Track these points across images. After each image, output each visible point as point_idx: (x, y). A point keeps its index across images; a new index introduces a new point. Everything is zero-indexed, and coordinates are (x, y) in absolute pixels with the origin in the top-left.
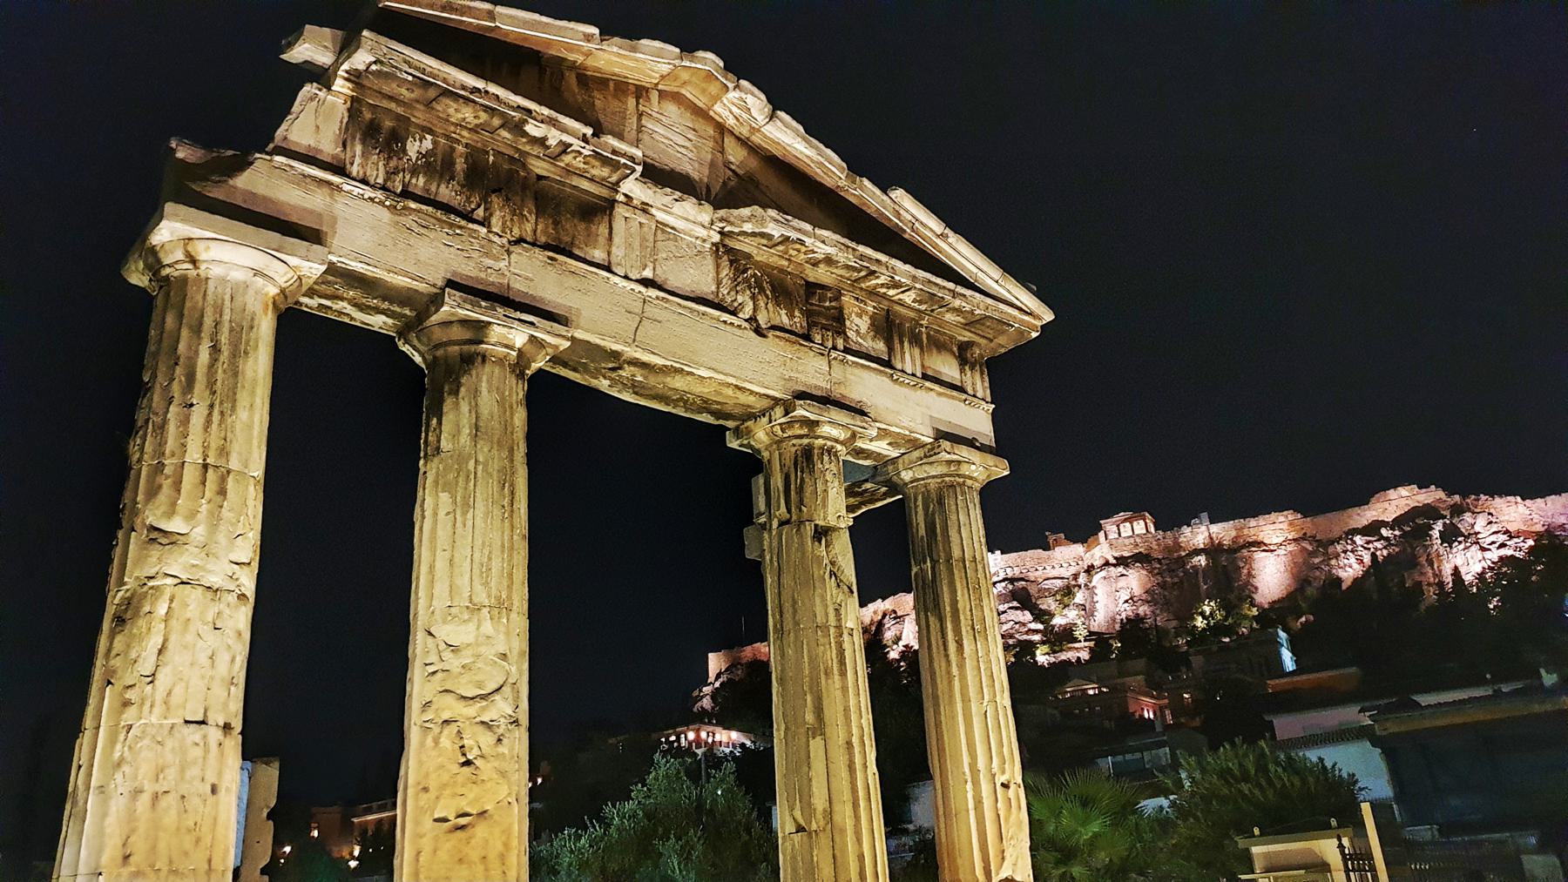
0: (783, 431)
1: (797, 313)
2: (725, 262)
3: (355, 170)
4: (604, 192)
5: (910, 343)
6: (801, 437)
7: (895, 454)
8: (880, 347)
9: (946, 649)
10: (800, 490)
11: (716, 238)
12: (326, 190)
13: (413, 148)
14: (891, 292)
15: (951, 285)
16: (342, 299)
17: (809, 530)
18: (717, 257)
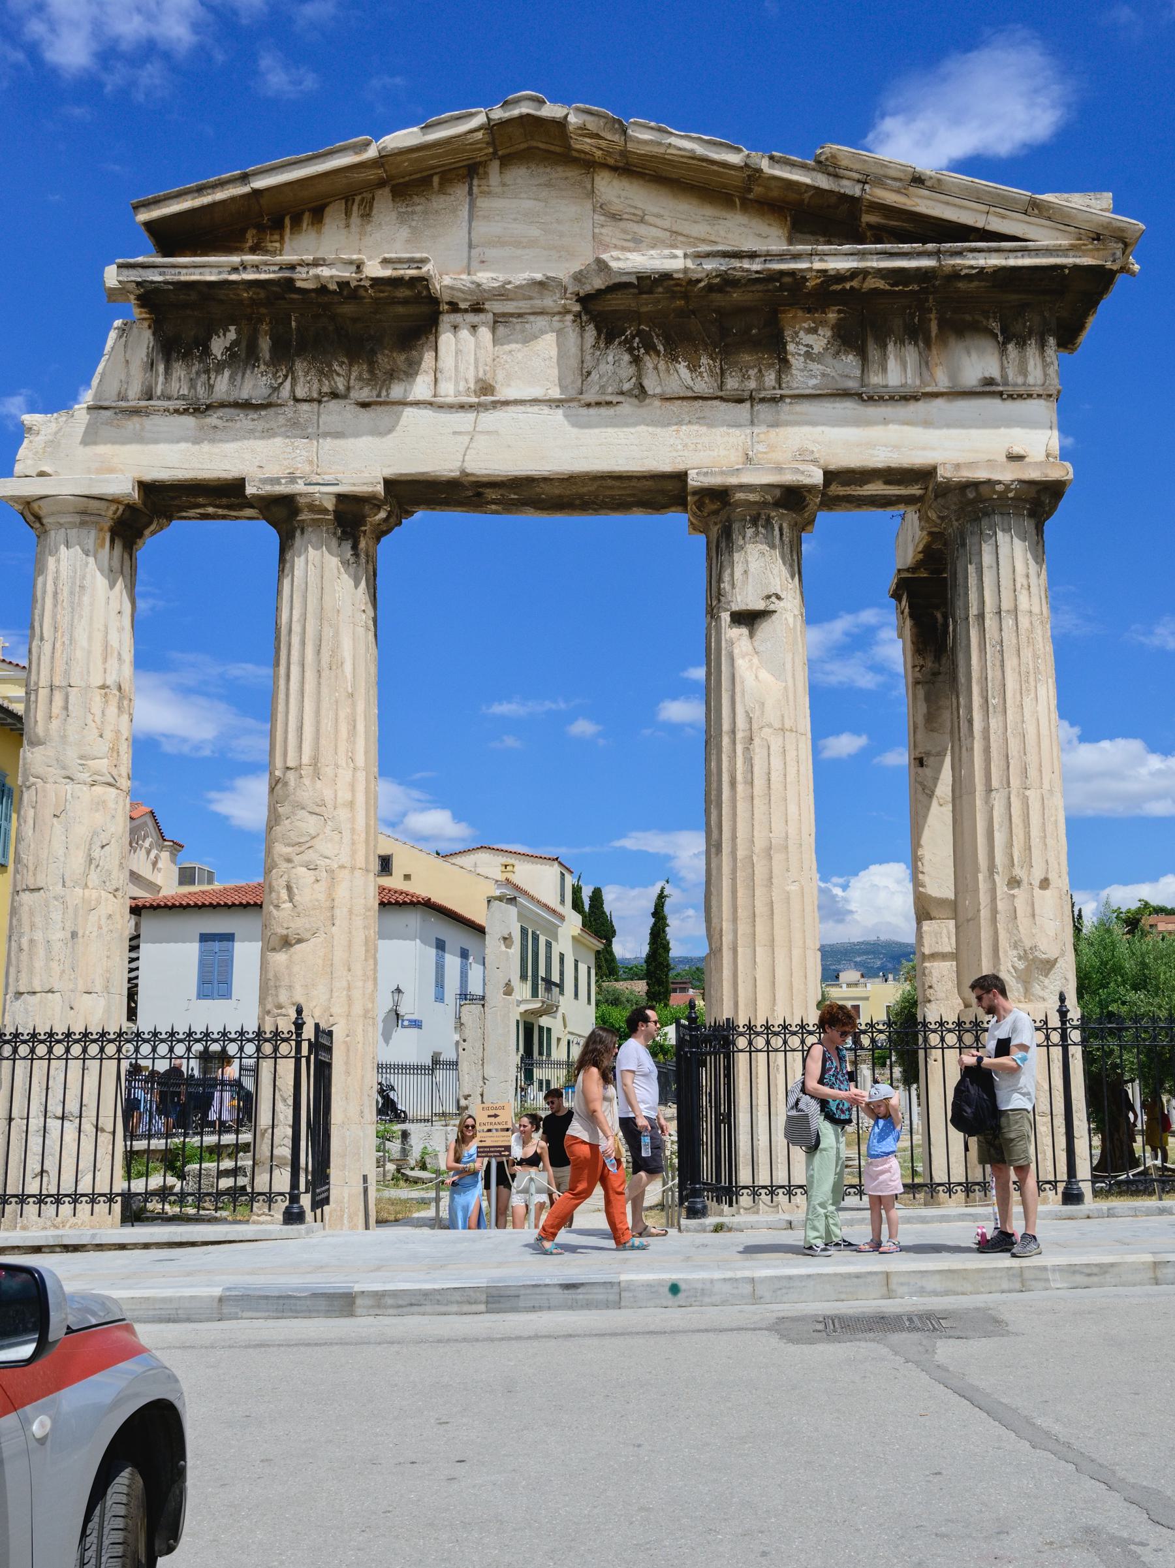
1: (704, 360)
2: (591, 332)
3: (159, 391)
4: (425, 309)
6: (716, 513)
8: (850, 360)
11: (577, 308)
12: (136, 419)
13: (218, 346)
17: (725, 617)
18: (582, 329)
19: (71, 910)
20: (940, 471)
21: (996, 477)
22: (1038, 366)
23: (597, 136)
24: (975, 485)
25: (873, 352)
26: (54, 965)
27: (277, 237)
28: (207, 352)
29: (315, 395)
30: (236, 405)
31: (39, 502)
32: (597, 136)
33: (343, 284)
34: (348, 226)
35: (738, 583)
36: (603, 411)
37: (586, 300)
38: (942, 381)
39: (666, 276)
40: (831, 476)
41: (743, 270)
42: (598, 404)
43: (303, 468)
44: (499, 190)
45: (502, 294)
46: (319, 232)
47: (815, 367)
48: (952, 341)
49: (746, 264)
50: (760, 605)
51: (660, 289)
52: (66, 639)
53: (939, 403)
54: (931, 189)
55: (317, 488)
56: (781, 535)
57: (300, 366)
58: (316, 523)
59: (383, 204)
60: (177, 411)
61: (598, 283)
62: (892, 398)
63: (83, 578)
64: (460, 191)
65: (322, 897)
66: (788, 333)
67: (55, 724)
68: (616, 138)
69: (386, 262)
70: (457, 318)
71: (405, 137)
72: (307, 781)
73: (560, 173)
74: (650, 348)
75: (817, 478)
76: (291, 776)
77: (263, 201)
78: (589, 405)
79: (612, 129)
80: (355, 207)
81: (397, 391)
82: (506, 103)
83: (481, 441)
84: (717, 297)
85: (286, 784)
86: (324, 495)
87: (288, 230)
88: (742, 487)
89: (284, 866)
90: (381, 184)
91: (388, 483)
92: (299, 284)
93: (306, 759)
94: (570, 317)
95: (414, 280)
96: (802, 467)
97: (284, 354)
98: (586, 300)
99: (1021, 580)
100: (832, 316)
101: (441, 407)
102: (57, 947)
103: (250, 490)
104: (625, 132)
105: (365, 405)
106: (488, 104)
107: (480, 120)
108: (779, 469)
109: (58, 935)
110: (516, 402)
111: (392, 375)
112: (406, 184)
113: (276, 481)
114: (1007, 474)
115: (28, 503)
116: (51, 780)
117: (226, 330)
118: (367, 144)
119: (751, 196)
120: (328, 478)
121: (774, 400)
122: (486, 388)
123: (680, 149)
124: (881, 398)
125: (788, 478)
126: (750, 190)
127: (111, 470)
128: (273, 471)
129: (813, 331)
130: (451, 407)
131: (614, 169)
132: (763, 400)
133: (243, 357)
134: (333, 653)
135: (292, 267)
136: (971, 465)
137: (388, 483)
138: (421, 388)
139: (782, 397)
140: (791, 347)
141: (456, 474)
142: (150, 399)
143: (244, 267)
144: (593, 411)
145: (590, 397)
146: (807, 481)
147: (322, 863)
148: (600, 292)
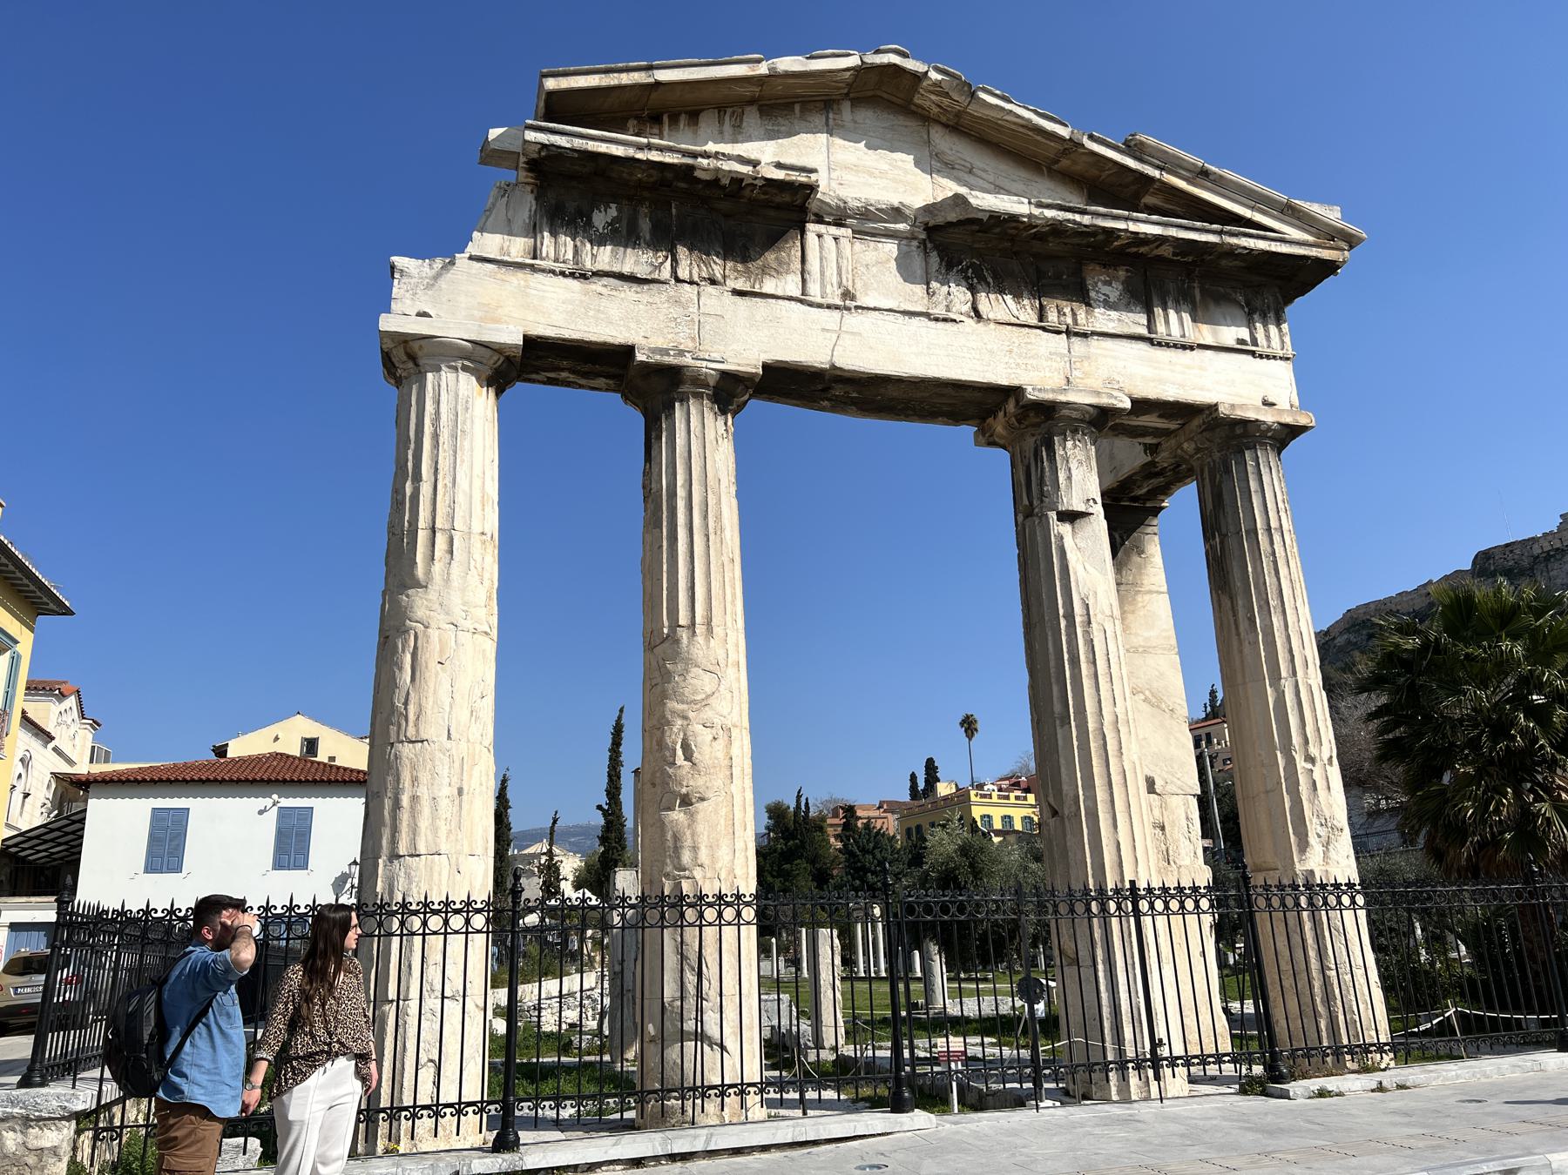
0: (1019, 422)
2: (934, 258)
5: (1177, 302)
7: (1173, 426)
9: (1237, 628)
10: (1041, 482)
11: (923, 236)
13: (600, 219)
14: (1142, 250)
16: (563, 370)
17: (1053, 515)
19: (457, 765)
20: (1221, 409)
21: (1261, 418)
22: (1273, 337)
23: (947, 95)
24: (1245, 422)
25: (1158, 311)
26: (441, 823)
27: (656, 131)
28: (589, 223)
29: (696, 279)
30: (621, 277)
31: (422, 342)
32: (947, 95)
33: (737, 180)
34: (721, 132)
35: (1062, 487)
36: (949, 325)
37: (931, 230)
38: (1209, 341)
39: (1014, 218)
40: (1134, 402)
41: (1074, 222)
42: (945, 320)
43: (687, 344)
44: (849, 125)
45: (865, 214)
46: (695, 132)
48: (1212, 306)
49: (1077, 217)
50: (1081, 508)
51: (997, 230)
52: (448, 480)
54: (1213, 182)
55: (704, 364)
57: (682, 252)
58: (699, 396)
59: (752, 118)
60: (563, 274)
61: (952, 217)
62: (1175, 346)
63: (464, 423)
64: (818, 120)
65: (721, 755)
66: (1089, 282)
67: (437, 567)
68: (961, 99)
69: (779, 166)
70: (822, 228)
71: (789, 63)
72: (700, 639)
73: (901, 120)
74: (982, 279)
76: (684, 635)
77: (654, 95)
78: (937, 320)
79: (961, 92)
80: (727, 118)
81: (769, 286)
82: (878, 52)
83: (846, 340)
84: (1037, 246)
85: (677, 641)
86: (708, 368)
87: (666, 127)
88: (1068, 403)
89: (679, 722)
90: (751, 102)
91: (765, 366)
92: (697, 174)
93: (698, 619)
94: (915, 243)
95: (803, 186)
96: (1115, 393)
97: (664, 239)
98: (931, 230)
99: (1281, 505)
100: (1122, 273)
101: (811, 304)
102: (444, 804)
103: (640, 357)
104: (973, 95)
106: (863, 51)
107: (853, 61)
108: (1098, 393)
109: (446, 792)
110: (875, 309)
111: (765, 271)
112: (772, 107)
113: (665, 352)
114: (1268, 417)
115: (406, 342)
116: (433, 625)
117: (607, 207)
118: (759, 61)
119: (1056, 167)
120: (716, 356)
121: (1085, 335)
122: (847, 295)
123: (1018, 116)
124: (1168, 345)
125: (1104, 401)
126: (1057, 162)
127: (497, 321)
128: (661, 343)
129: (1108, 283)
130: (820, 306)
131: (946, 126)
132: (1077, 334)
133: (623, 235)
134: (719, 518)
135: (695, 155)
136: (1242, 406)
137: (765, 366)
138: (791, 285)
139: (1094, 333)
140: (1092, 294)
142: (535, 258)
143: (649, 147)
144: (940, 325)
145: (939, 311)
146: (1120, 405)
147: (718, 721)
148: (950, 224)
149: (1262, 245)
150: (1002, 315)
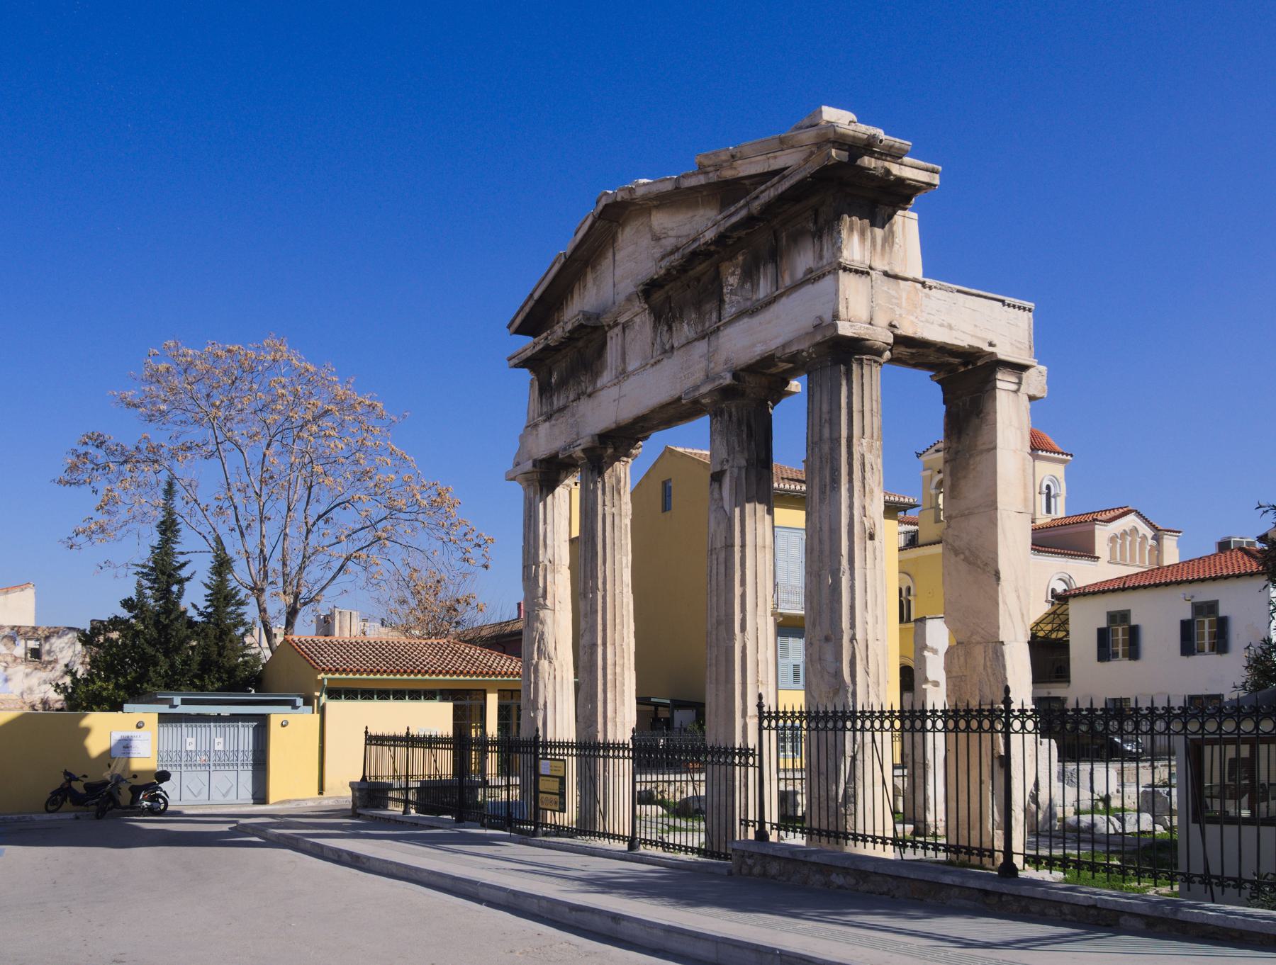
15: (742, 202)
21: (801, 347)
36: (658, 366)
38: (787, 281)
47: (734, 298)
53: (784, 299)
56: (730, 417)
74: (674, 317)
75: (728, 380)
81: (599, 384)
105: (590, 396)
111: (596, 374)
114: (805, 345)
122: (624, 371)
129: (733, 274)
138: (606, 377)
141: (613, 426)
149: (772, 193)
150: (683, 341)
